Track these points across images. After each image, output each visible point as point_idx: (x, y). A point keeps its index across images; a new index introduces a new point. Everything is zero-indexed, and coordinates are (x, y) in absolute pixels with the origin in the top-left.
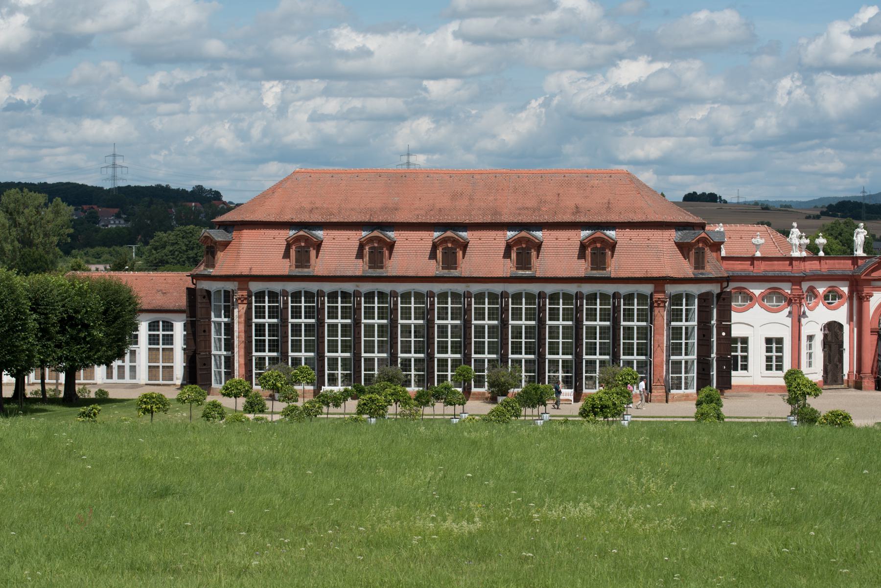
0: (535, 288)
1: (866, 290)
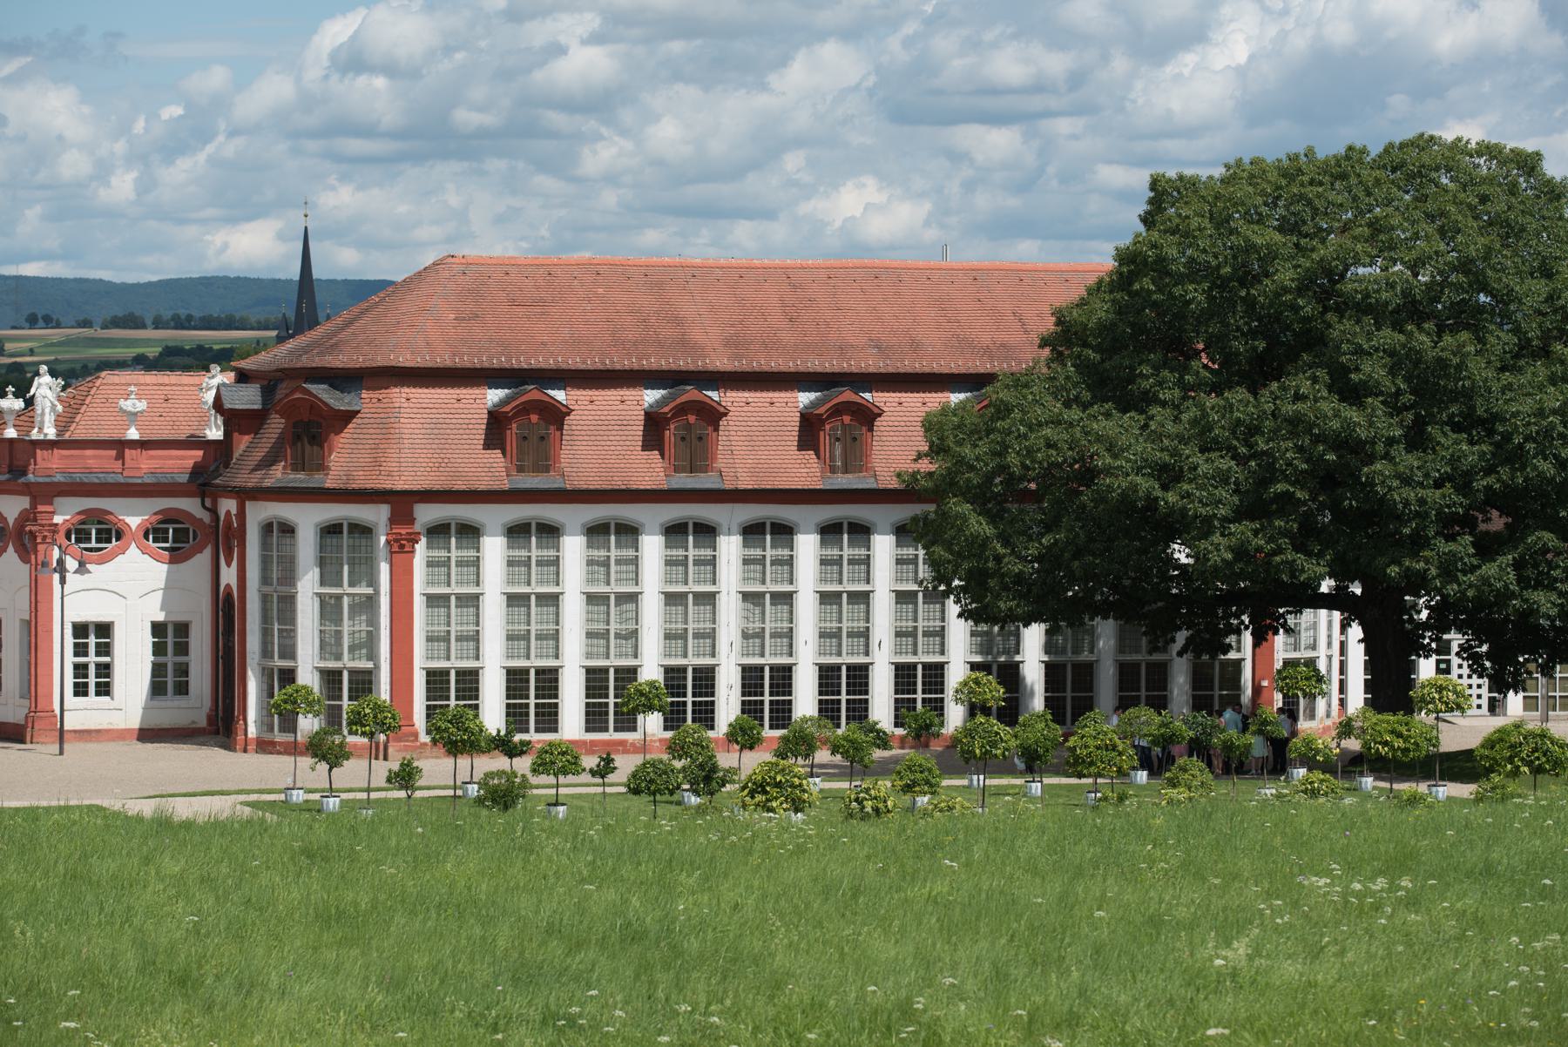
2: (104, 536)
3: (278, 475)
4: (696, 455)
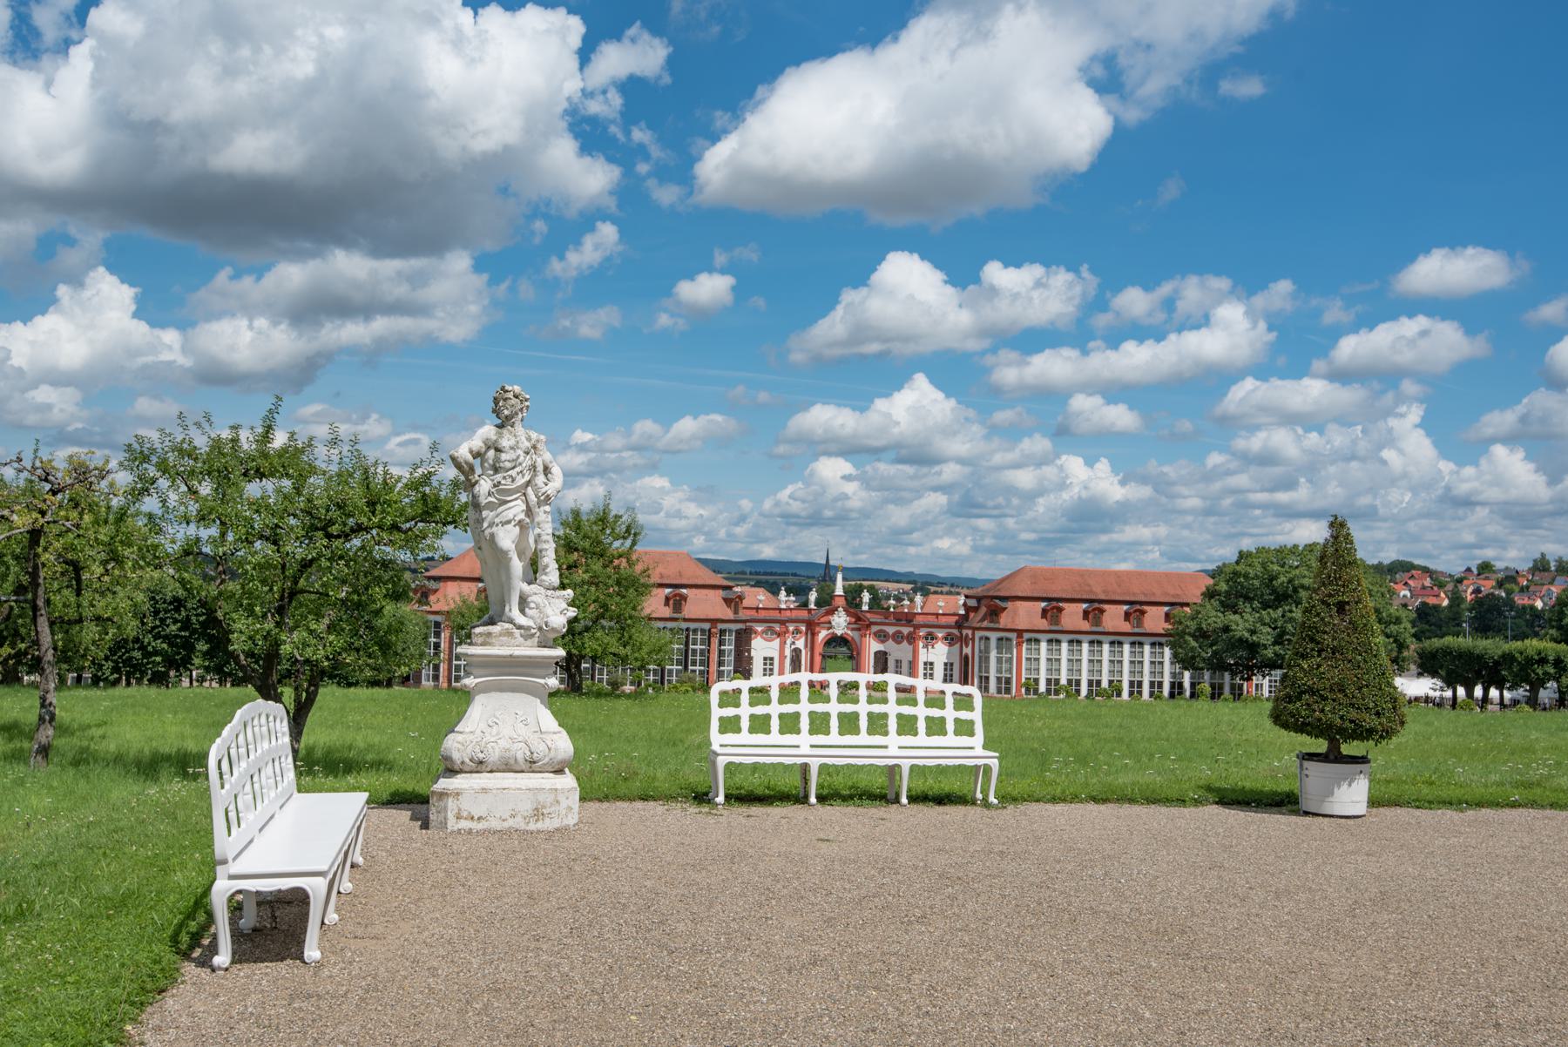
0: (684, 625)
1: (817, 629)
2: (932, 639)
3: (985, 624)
4: (1098, 622)
